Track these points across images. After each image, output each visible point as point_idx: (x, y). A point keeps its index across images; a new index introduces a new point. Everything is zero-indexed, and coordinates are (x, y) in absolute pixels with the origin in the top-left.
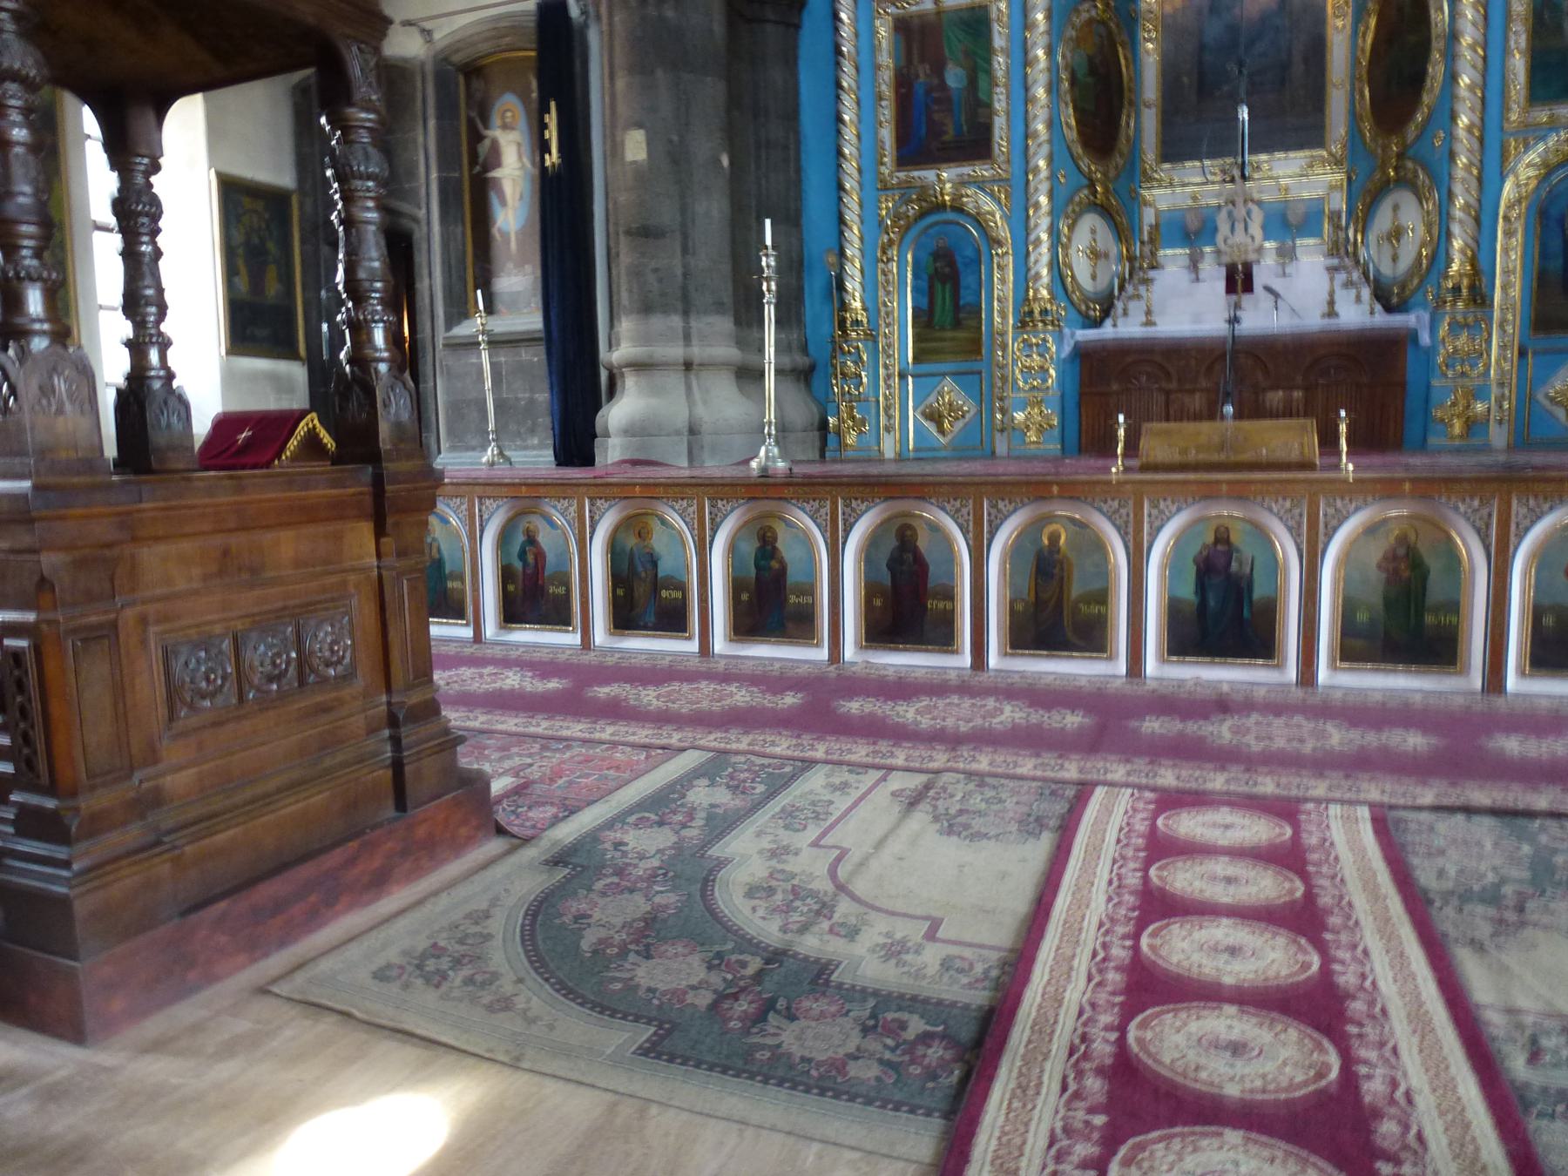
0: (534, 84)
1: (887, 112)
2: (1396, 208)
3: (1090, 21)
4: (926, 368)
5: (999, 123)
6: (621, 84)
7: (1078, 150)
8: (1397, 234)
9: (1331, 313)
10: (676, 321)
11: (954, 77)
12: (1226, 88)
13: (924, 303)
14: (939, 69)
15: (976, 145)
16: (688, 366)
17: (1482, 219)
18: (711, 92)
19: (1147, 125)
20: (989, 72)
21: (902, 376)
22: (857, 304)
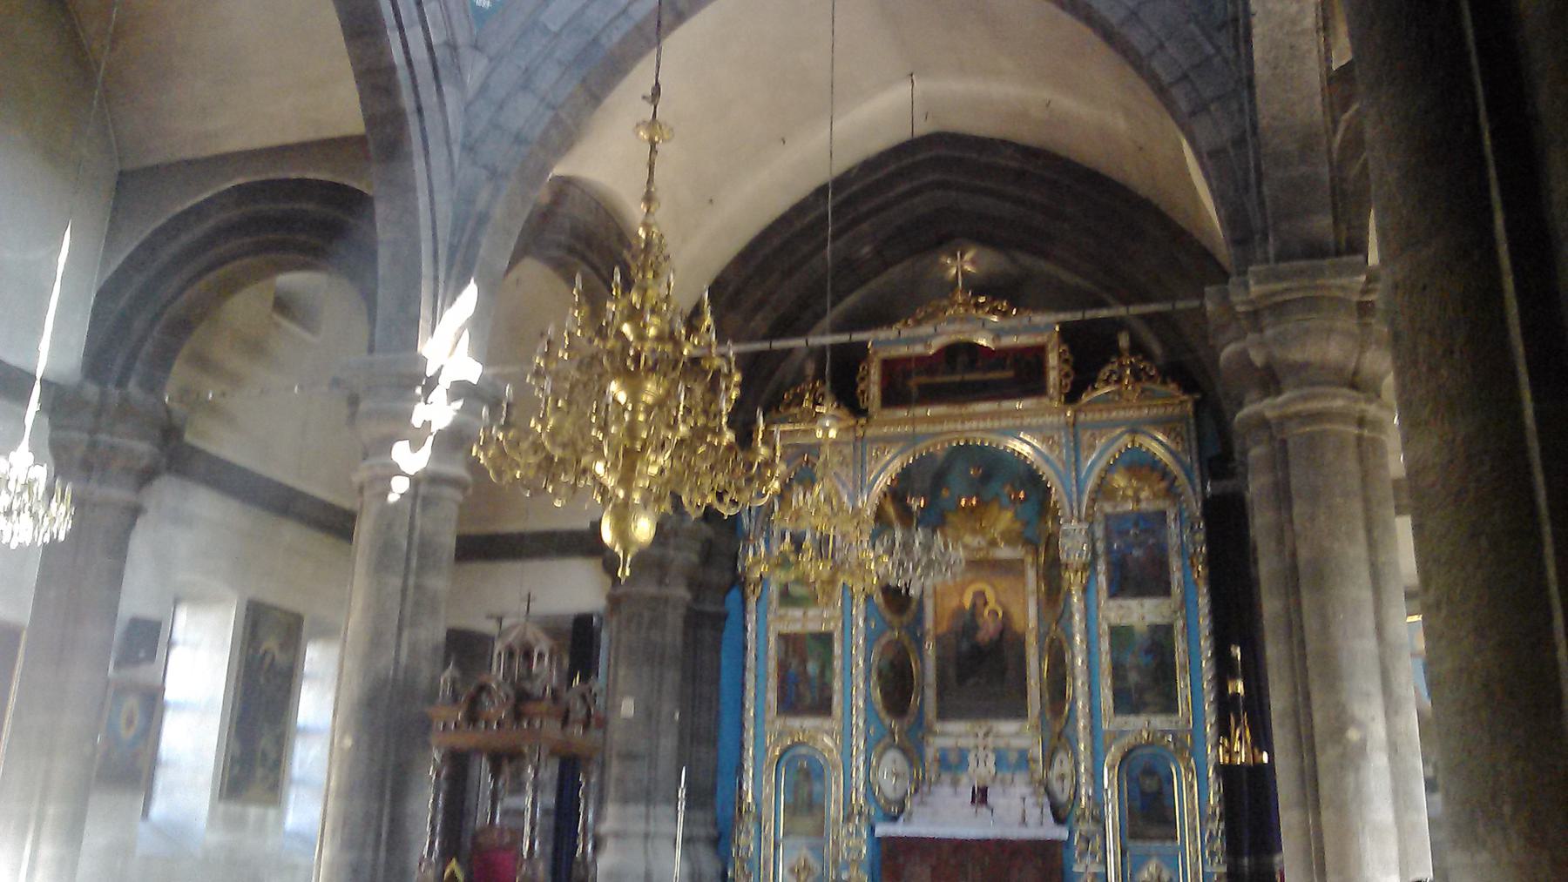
1: (773, 683)
2: (1062, 762)
3: (889, 643)
4: (791, 841)
5: (836, 699)
6: (622, 672)
7: (883, 714)
8: (1062, 777)
9: (1024, 821)
10: (642, 809)
11: (812, 668)
12: (971, 682)
13: (792, 800)
14: (804, 662)
15: (822, 707)
16: (647, 836)
17: (1096, 776)
18: (672, 676)
19: (928, 697)
20: (832, 670)
21: (776, 847)
22: (750, 799)
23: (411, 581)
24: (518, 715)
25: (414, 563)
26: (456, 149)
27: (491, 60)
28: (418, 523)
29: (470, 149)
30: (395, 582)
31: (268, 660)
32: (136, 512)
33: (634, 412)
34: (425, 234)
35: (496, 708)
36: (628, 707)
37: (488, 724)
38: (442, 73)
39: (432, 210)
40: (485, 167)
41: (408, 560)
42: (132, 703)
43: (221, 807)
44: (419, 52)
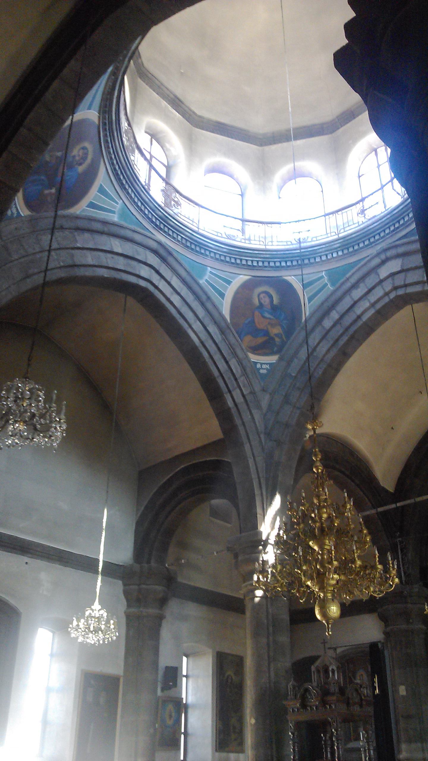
0: (369, 667)
6: (397, 672)
23: (271, 638)
24: (324, 703)
25: (271, 629)
26: (262, 436)
27: (270, 394)
28: (270, 611)
29: (268, 434)
30: (264, 640)
31: (229, 681)
32: (161, 618)
33: (322, 555)
34: (254, 476)
35: (314, 701)
36: (402, 690)
37: (312, 709)
38: (251, 405)
39: (256, 465)
40: (275, 441)
41: (268, 629)
42: (170, 707)
43: (217, 754)
44: (239, 399)
